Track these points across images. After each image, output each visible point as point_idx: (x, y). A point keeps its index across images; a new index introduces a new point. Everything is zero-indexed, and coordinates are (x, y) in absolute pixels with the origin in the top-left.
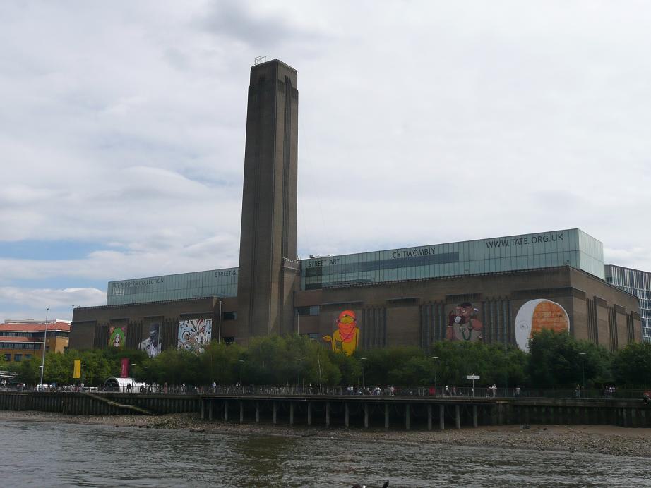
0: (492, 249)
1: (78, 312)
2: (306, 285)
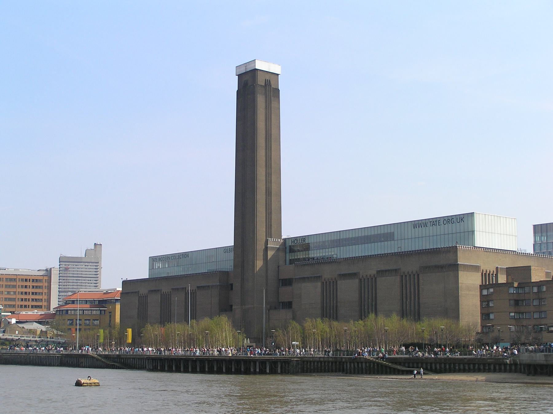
0: (417, 229)
1: (125, 283)
2: (290, 260)
